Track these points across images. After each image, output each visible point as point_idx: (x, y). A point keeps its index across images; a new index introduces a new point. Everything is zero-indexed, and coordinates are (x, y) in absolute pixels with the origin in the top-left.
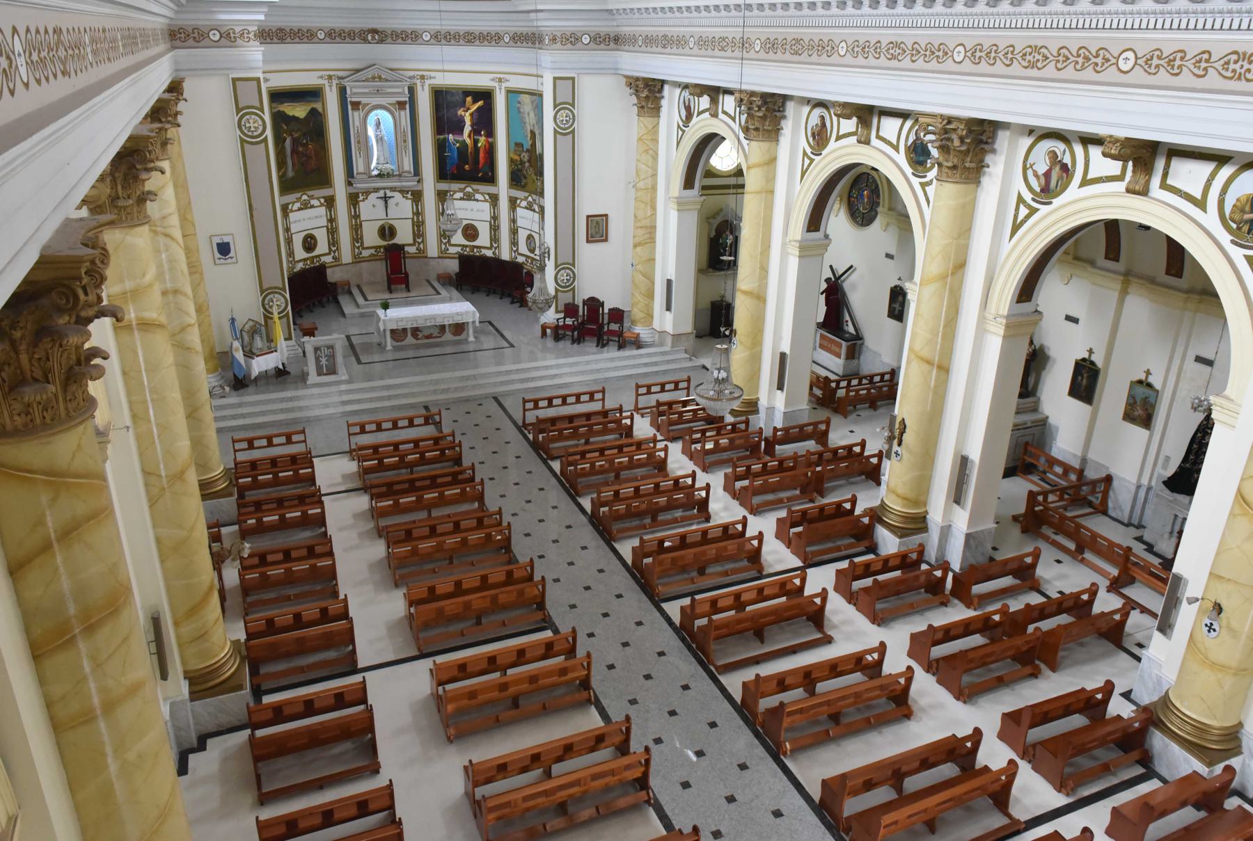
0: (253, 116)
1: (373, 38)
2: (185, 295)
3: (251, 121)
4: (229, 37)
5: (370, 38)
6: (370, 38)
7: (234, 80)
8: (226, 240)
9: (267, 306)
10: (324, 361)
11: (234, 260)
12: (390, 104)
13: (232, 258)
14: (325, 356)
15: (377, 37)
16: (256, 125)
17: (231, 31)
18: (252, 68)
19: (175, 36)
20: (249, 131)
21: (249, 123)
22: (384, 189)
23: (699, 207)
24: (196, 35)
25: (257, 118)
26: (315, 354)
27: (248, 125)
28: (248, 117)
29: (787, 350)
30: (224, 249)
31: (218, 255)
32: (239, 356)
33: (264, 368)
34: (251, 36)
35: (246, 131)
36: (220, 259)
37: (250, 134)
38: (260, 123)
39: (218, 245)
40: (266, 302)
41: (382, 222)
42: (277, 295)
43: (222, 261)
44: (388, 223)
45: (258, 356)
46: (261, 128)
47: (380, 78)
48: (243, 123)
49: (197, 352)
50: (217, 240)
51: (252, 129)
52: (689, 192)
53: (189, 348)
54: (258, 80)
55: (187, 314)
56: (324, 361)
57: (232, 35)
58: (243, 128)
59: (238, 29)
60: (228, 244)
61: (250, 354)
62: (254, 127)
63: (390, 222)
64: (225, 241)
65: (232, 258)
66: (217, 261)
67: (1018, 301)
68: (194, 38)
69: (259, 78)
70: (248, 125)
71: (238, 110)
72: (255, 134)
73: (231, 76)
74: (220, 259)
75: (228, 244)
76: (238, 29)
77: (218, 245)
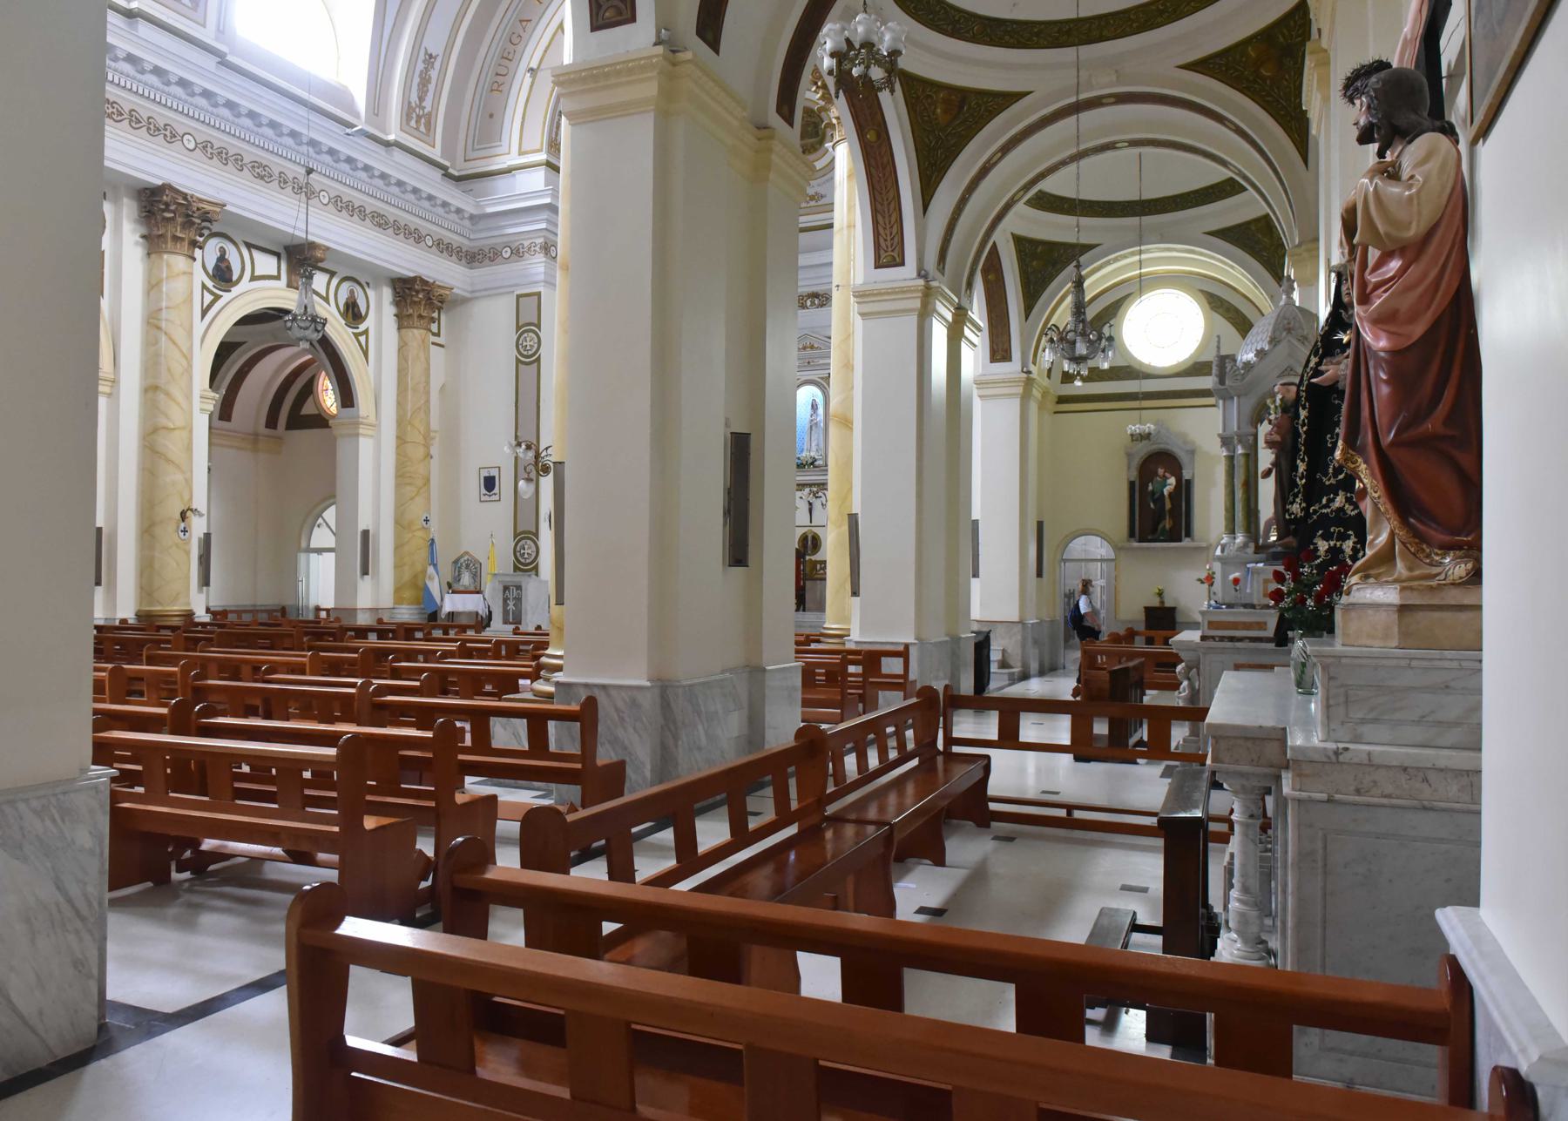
0: (531, 334)
1: (813, 303)
2: (168, 394)
3: (528, 339)
4: (517, 253)
5: (809, 303)
6: (809, 303)
7: (518, 297)
8: (494, 473)
9: (518, 554)
10: (511, 607)
11: (497, 498)
12: (822, 378)
13: (495, 494)
14: (514, 599)
15: (816, 302)
16: (531, 343)
17: (521, 247)
18: (536, 282)
19: (475, 257)
20: (525, 350)
21: (526, 341)
22: (810, 485)
23: (1020, 390)
24: (491, 255)
25: (534, 335)
26: (504, 592)
27: (525, 344)
28: (526, 335)
29: (856, 509)
30: (490, 483)
31: (484, 491)
32: (435, 587)
33: (460, 608)
34: (537, 248)
35: (522, 350)
36: (484, 495)
37: (525, 353)
38: (536, 341)
39: (485, 478)
40: (518, 548)
41: (805, 530)
42: (529, 542)
43: (487, 498)
44: (812, 531)
45: (453, 592)
46: (536, 346)
47: (812, 347)
48: (520, 342)
49: (168, 460)
50: (485, 473)
51: (528, 348)
52: (1002, 368)
53: (157, 452)
54: (539, 294)
55: (167, 416)
56: (511, 607)
57: (521, 250)
58: (520, 346)
59: (526, 243)
60: (494, 477)
61: (452, 588)
62: (530, 346)
63: (813, 529)
64: (492, 475)
65: (495, 494)
66: (483, 498)
67: (595, 28)
68: (490, 257)
69: (540, 292)
70: (525, 344)
71: (518, 328)
72: (530, 353)
73: (516, 293)
74: (484, 495)
75: (494, 477)
76: (526, 243)
77: (485, 478)
